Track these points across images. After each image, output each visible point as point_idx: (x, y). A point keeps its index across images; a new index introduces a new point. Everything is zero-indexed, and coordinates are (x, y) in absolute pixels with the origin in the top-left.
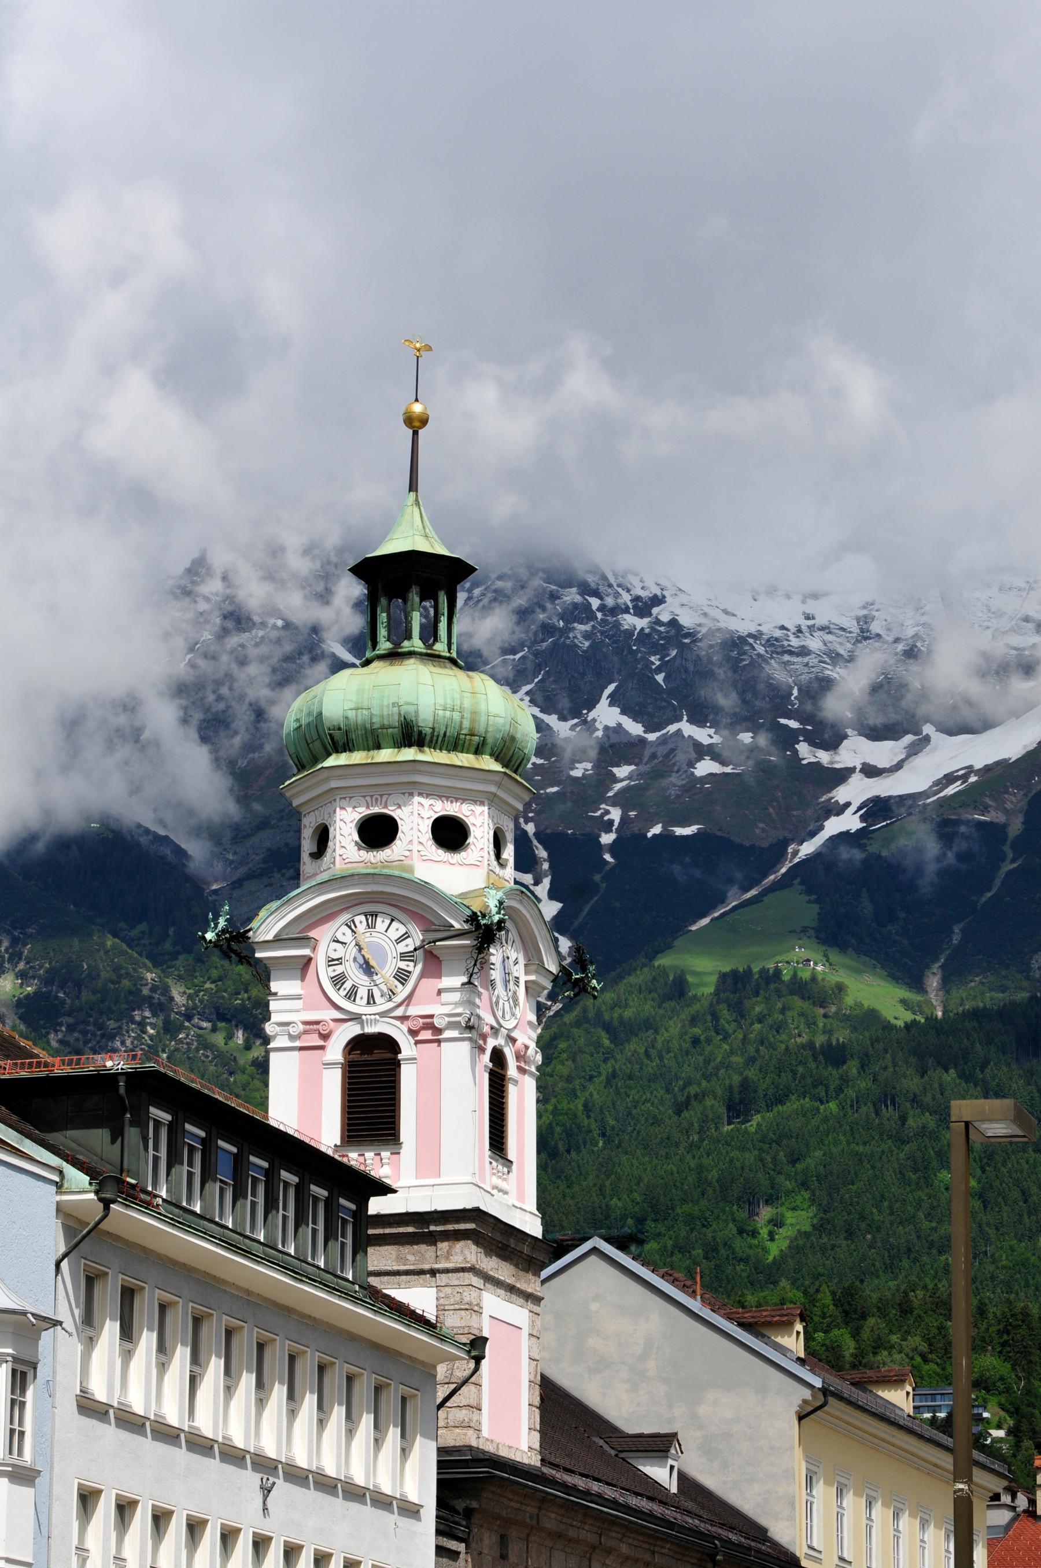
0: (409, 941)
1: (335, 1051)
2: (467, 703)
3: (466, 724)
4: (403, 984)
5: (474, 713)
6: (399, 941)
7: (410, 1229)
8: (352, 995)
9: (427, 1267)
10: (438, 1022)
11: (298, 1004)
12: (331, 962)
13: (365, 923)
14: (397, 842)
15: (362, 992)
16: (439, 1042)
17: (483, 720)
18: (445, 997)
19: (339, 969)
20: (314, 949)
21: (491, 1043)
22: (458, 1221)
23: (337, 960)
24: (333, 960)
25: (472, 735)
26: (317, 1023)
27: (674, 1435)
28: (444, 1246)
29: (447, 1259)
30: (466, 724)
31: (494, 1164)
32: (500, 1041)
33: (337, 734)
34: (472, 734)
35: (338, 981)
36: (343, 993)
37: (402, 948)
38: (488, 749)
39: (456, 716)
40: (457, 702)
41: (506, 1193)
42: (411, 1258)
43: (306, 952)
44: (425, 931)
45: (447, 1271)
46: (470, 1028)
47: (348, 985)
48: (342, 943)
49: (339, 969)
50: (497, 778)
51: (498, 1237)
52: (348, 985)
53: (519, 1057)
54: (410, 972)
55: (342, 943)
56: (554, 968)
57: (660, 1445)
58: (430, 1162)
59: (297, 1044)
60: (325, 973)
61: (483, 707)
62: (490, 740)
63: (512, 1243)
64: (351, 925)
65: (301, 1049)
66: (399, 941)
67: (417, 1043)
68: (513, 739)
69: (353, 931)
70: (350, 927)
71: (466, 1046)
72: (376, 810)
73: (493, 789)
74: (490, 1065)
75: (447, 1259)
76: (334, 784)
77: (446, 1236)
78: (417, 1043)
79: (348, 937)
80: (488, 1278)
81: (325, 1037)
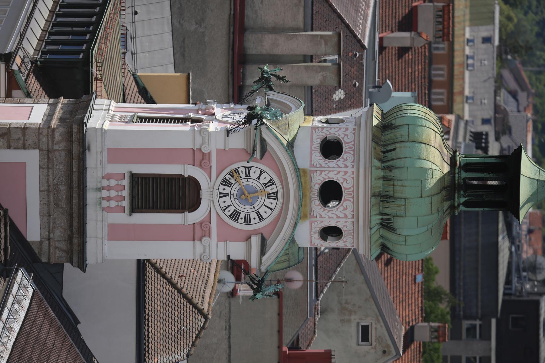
0: (257, 220)
4: (230, 216)
6: (258, 214)
12: (248, 169)
13: (271, 191)
19: (243, 175)
23: (249, 174)
24: (249, 171)
48: (259, 177)
49: (243, 175)
54: (237, 220)
55: (259, 177)
66: (258, 214)
69: (267, 184)
70: (269, 182)
79: (262, 181)
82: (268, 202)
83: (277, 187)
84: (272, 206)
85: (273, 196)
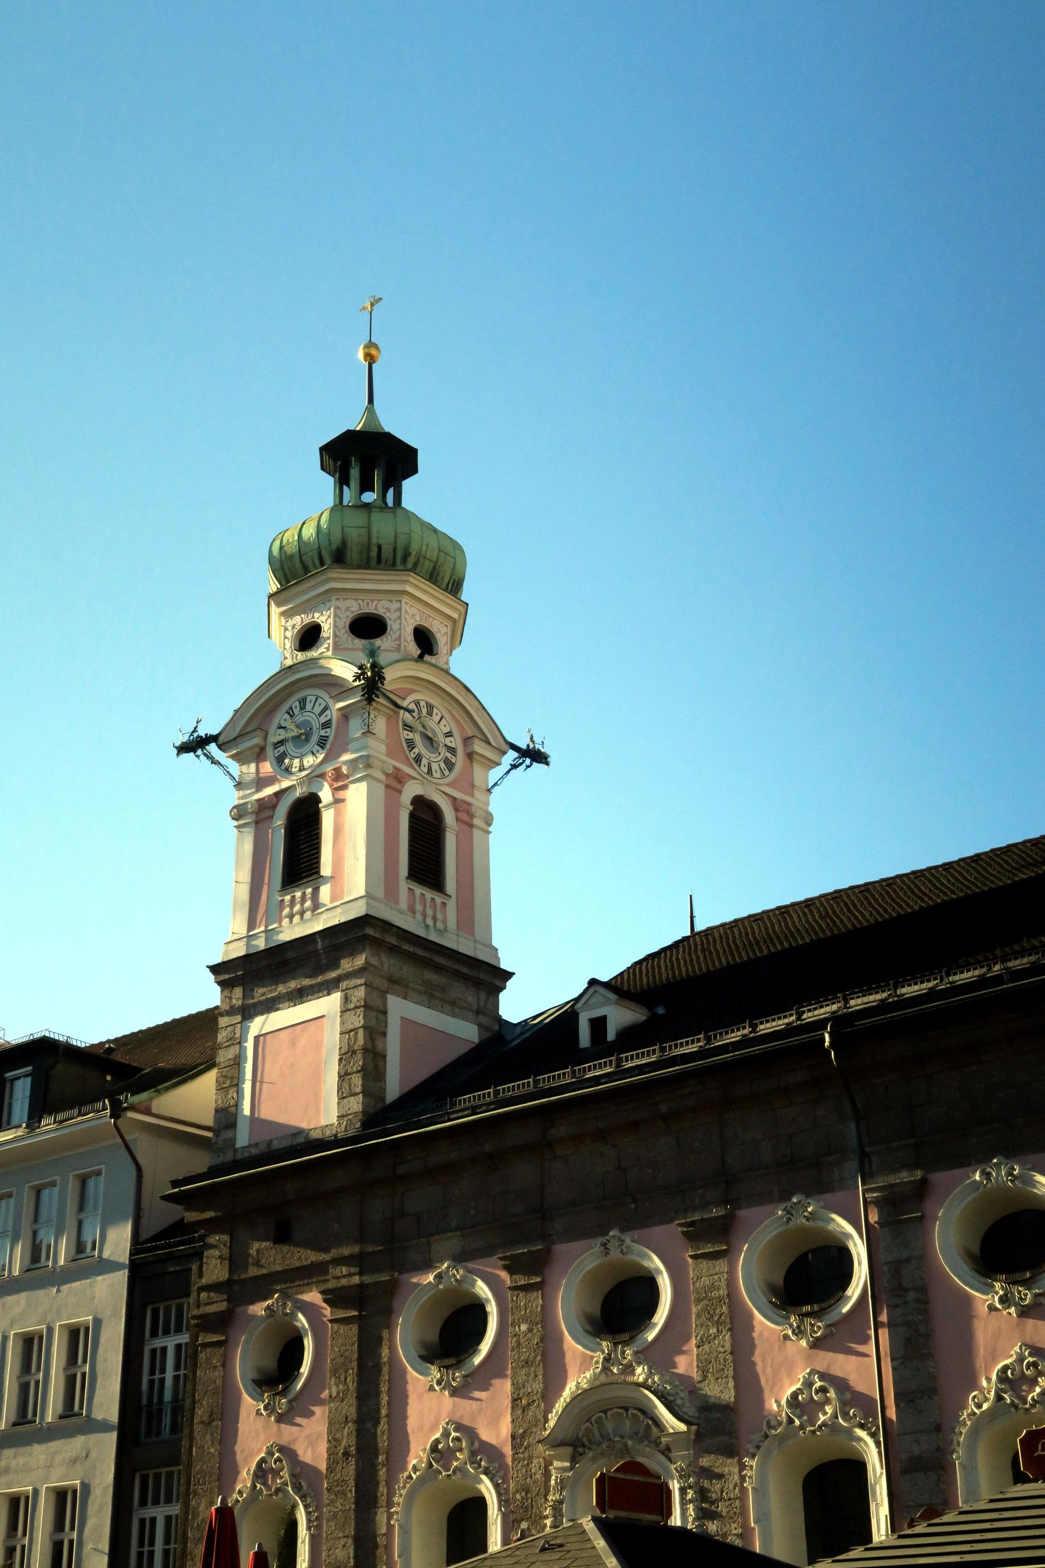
19: (282, 749)
21: (411, 790)
37: (323, 719)
70: (288, 713)
74: (411, 808)
81: (274, 807)
82: (309, 706)
83: (294, 702)
84: (314, 699)
85: (303, 702)
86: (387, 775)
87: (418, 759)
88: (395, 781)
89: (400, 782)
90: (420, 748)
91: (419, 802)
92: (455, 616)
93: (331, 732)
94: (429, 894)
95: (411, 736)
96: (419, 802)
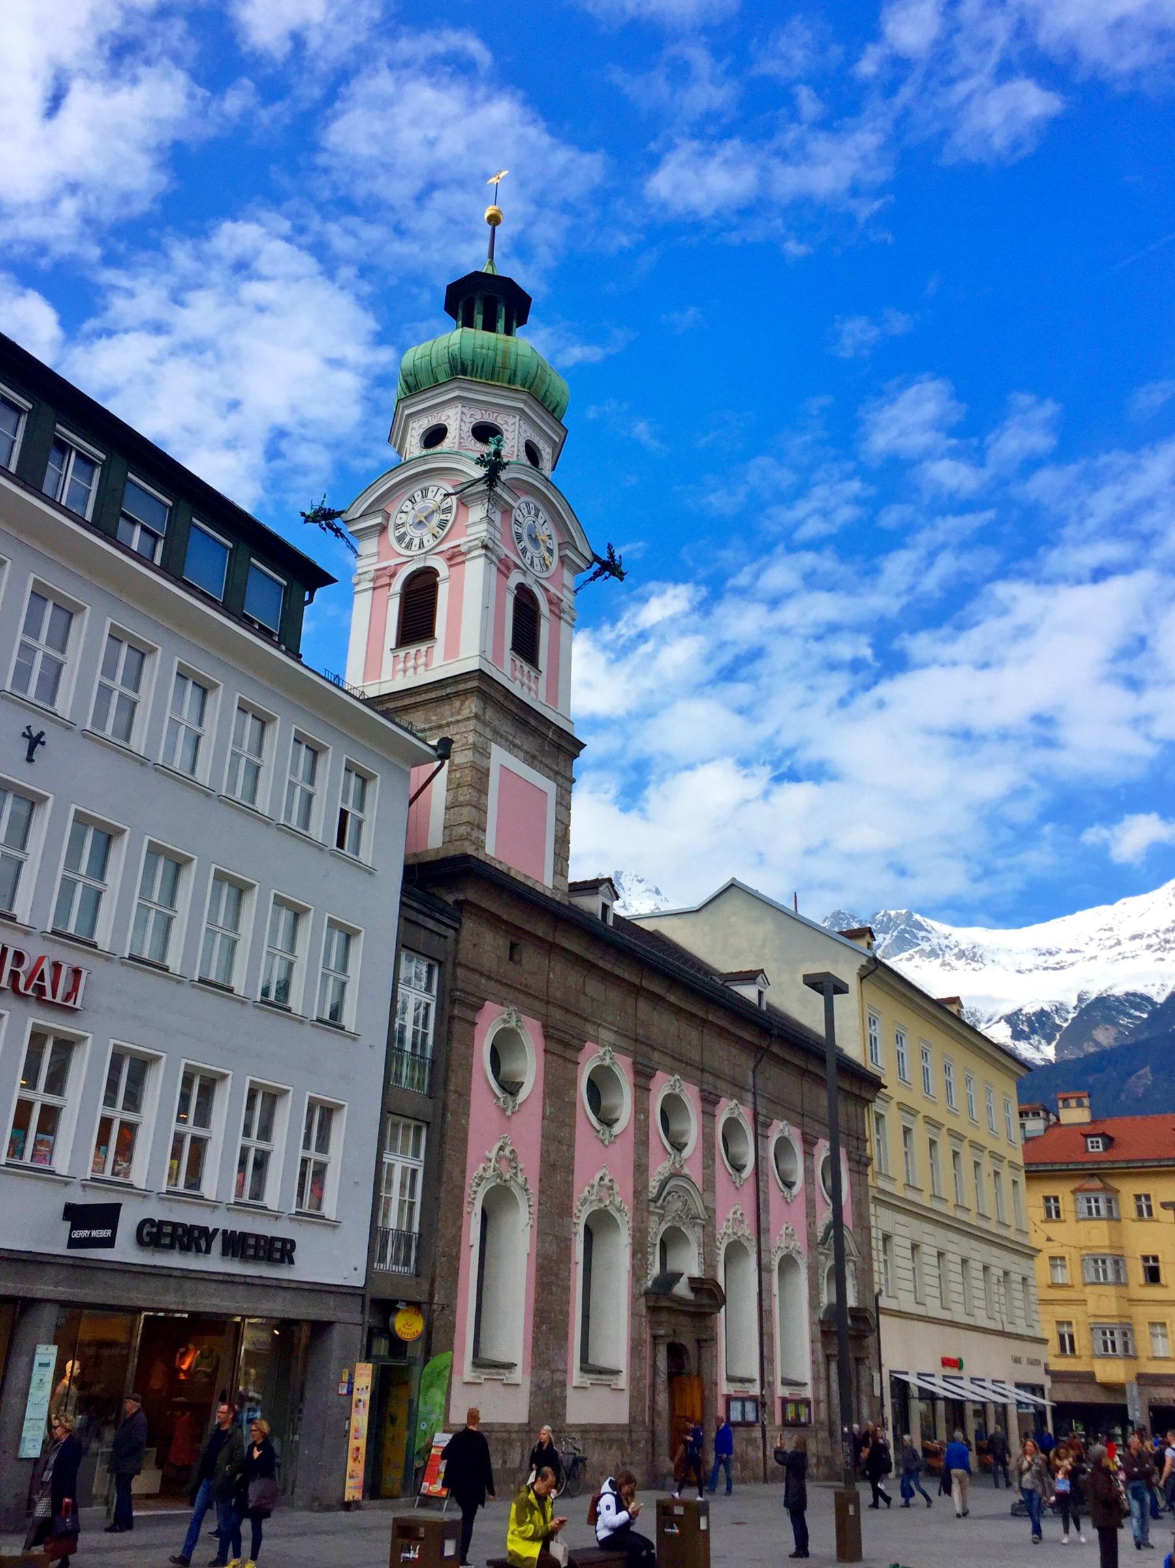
1: (397, 585)
2: (500, 346)
3: (499, 359)
5: (506, 354)
7: (433, 695)
8: (409, 546)
9: (444, 722)
10: (463, 549)
11: (375, 559)
12: (398, 526)
14: (446, 440)
15: (416, 542)
16: (463, 562)
17: (513, 357)
18: (470, 531)
19: (402, 530)
20: (388, 520)
21: (516, 578)
22: (466, 681)
25: (504, 368)
26: (385, 568)
27: (762, 971)
28: (457, 704)
29: (459, 713)
30: (499, 359)
31: (518, 663)
32: (529, 582)
33: (411, 379)
34: (504, 368)
35: (400, 539)
36: (403, 545)
38: (519, 379)
39: (491, 353)
40: (492, 346)
41: (530, 689)
42: (434, 718)
43: (379, 520)
44: (454, 487)
45: (458, 721)
46: (485, 547)
47: (407, 540)
49: (402, 530)
50: (524, 397)
51: (513, 708)
52: (407, 540)
53: (550, 602)
56: (589, 557)
57: (750, 977)
58: (452, 650)
59: (371, 585)
60: (392, 534)
61: (513, 350)
62: (519, 374)
63: (532, 722)
64: (412, 500)
65: (374, 589)
67: (450, 566)
68: (543, 381)
71: (483, 559)
72: (434, 422)
73: (521, 405)
75: (459, 713)
76: (407, 412)
77: (457, 694)
78: (450, 566)
80: (498, 736)
81: (392, 576)
82: (430, 495)
84: (435, 489)
85: (424, 493)
86: (500, 560)
87: (524, 551)
88: (504, 568)
89: (508, 568)
90: (526, 542)
91: (521, 587)
92: (557, 439)
93: (451, 517)
94: (526, 668)
95: (520, 531)
96: (521, 587)
